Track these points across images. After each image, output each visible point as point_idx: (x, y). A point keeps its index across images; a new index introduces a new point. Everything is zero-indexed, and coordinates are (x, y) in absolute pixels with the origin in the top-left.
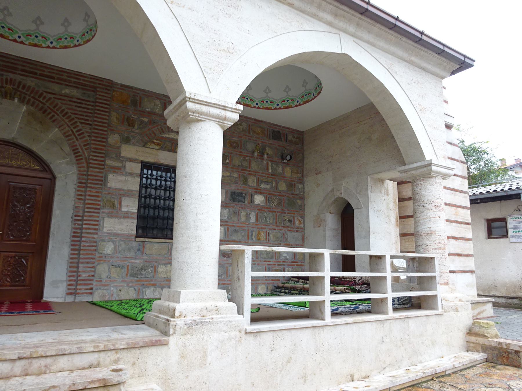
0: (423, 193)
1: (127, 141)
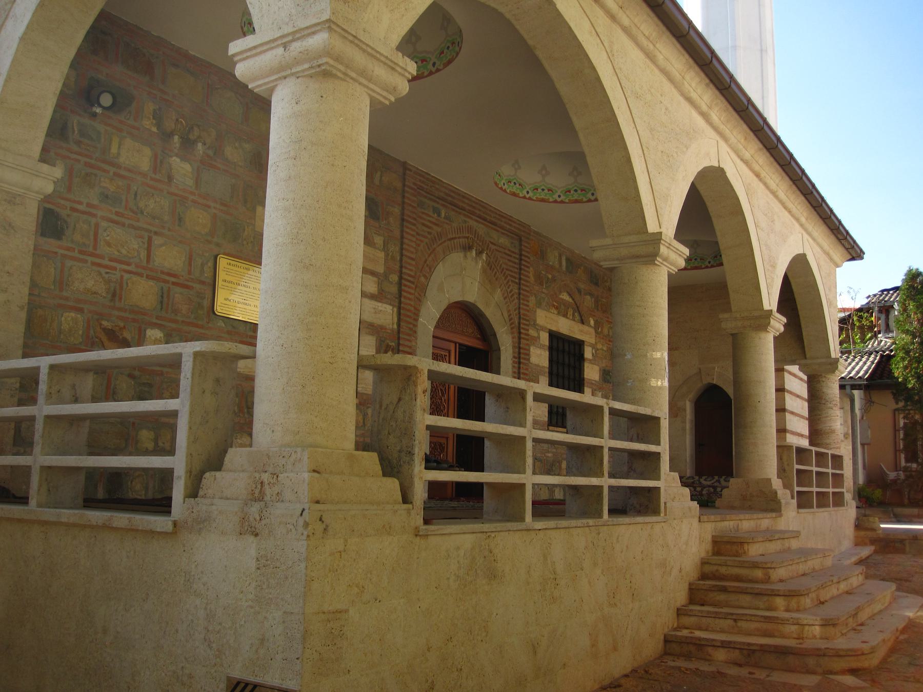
0: (825, 390)
1: (539, 304)
